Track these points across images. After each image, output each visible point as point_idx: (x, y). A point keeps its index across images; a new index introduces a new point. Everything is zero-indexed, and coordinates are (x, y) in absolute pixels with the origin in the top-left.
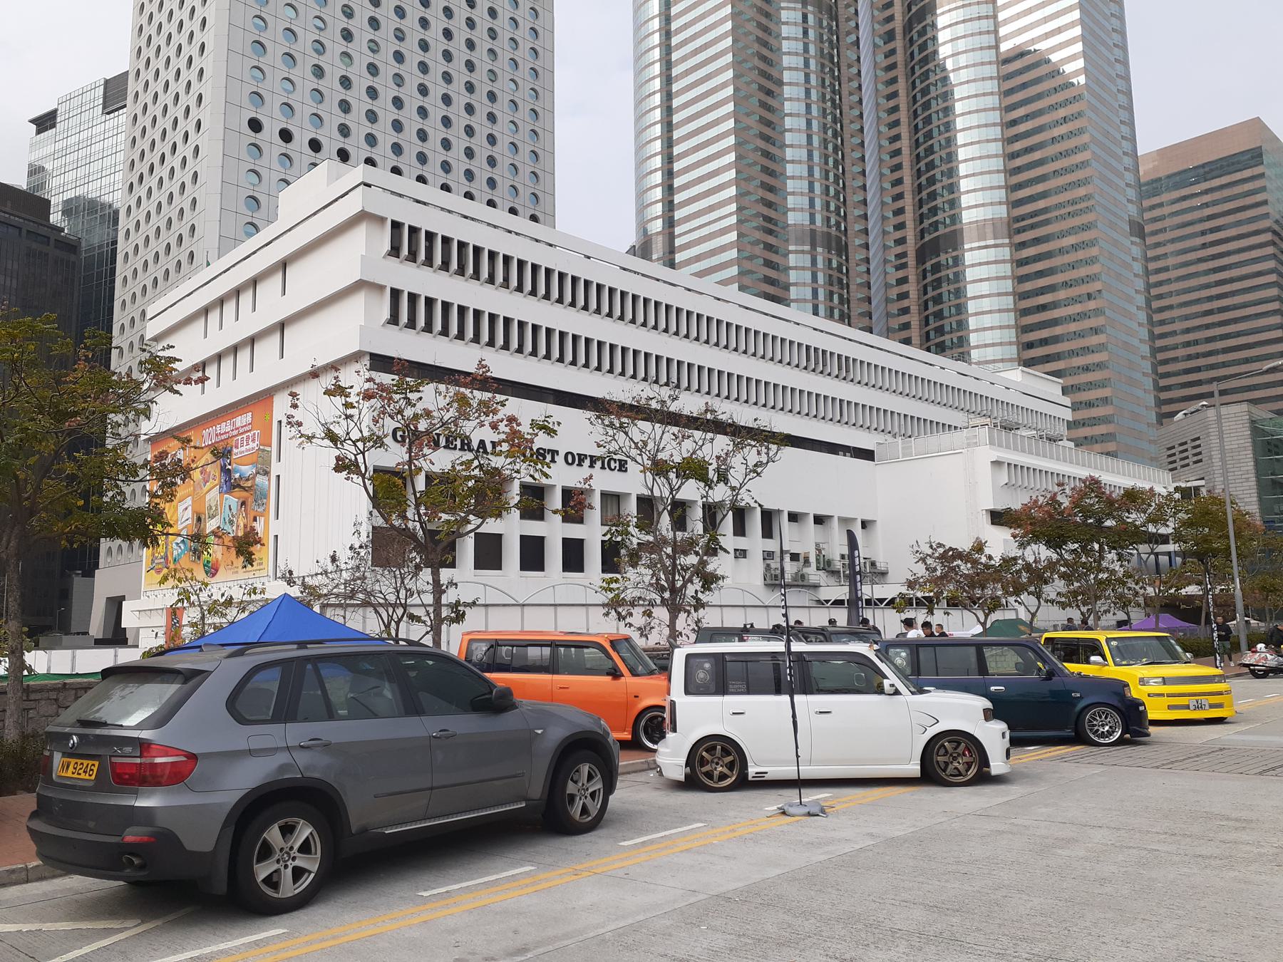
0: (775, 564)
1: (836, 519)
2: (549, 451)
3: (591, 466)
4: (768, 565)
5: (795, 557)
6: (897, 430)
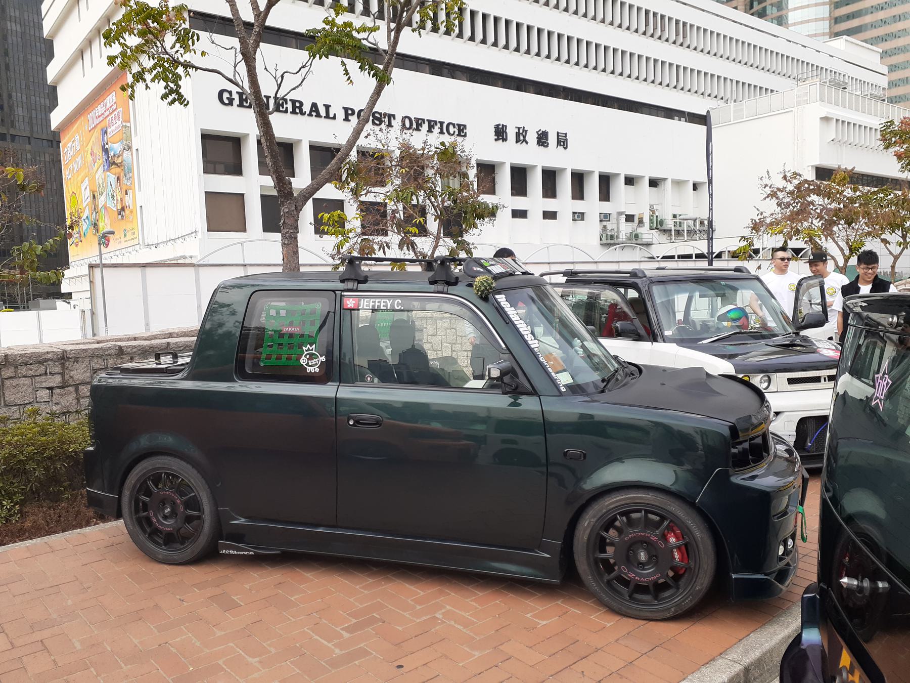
0: (610, 226)
1: (669, 181)
2: (385, 114)
3: (430, 131)
4: (605, 227)
5: (630, 218)
6: (729, 95)
